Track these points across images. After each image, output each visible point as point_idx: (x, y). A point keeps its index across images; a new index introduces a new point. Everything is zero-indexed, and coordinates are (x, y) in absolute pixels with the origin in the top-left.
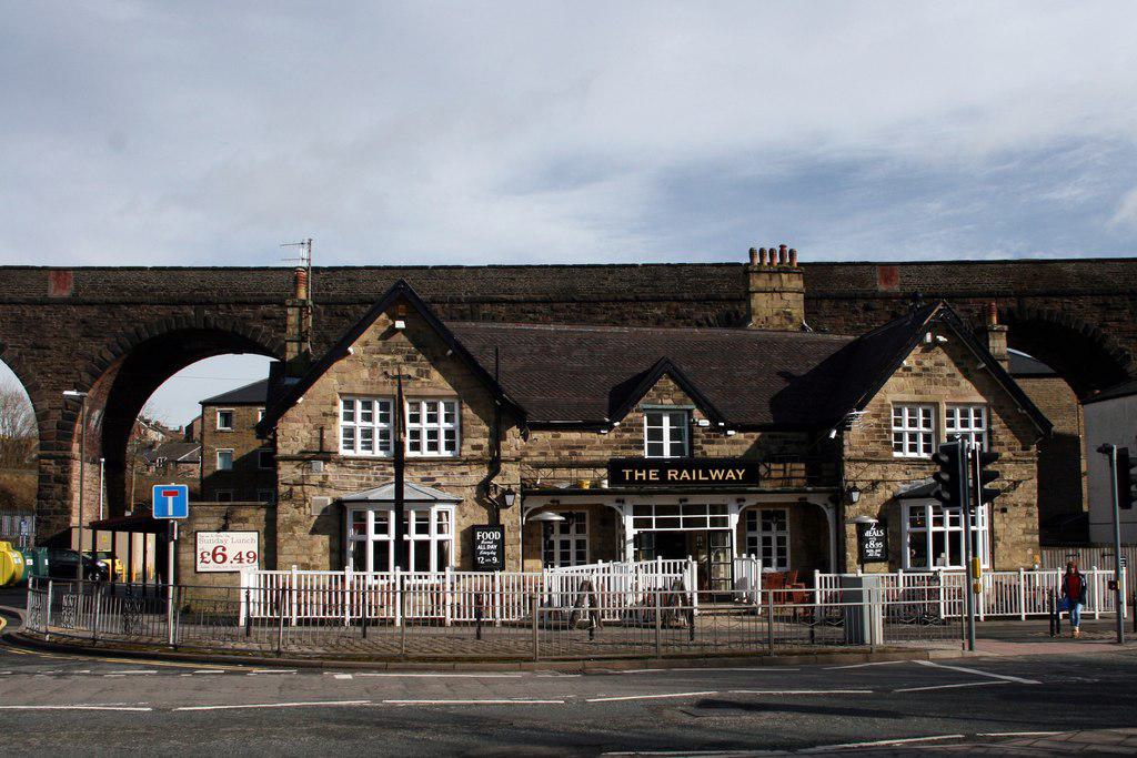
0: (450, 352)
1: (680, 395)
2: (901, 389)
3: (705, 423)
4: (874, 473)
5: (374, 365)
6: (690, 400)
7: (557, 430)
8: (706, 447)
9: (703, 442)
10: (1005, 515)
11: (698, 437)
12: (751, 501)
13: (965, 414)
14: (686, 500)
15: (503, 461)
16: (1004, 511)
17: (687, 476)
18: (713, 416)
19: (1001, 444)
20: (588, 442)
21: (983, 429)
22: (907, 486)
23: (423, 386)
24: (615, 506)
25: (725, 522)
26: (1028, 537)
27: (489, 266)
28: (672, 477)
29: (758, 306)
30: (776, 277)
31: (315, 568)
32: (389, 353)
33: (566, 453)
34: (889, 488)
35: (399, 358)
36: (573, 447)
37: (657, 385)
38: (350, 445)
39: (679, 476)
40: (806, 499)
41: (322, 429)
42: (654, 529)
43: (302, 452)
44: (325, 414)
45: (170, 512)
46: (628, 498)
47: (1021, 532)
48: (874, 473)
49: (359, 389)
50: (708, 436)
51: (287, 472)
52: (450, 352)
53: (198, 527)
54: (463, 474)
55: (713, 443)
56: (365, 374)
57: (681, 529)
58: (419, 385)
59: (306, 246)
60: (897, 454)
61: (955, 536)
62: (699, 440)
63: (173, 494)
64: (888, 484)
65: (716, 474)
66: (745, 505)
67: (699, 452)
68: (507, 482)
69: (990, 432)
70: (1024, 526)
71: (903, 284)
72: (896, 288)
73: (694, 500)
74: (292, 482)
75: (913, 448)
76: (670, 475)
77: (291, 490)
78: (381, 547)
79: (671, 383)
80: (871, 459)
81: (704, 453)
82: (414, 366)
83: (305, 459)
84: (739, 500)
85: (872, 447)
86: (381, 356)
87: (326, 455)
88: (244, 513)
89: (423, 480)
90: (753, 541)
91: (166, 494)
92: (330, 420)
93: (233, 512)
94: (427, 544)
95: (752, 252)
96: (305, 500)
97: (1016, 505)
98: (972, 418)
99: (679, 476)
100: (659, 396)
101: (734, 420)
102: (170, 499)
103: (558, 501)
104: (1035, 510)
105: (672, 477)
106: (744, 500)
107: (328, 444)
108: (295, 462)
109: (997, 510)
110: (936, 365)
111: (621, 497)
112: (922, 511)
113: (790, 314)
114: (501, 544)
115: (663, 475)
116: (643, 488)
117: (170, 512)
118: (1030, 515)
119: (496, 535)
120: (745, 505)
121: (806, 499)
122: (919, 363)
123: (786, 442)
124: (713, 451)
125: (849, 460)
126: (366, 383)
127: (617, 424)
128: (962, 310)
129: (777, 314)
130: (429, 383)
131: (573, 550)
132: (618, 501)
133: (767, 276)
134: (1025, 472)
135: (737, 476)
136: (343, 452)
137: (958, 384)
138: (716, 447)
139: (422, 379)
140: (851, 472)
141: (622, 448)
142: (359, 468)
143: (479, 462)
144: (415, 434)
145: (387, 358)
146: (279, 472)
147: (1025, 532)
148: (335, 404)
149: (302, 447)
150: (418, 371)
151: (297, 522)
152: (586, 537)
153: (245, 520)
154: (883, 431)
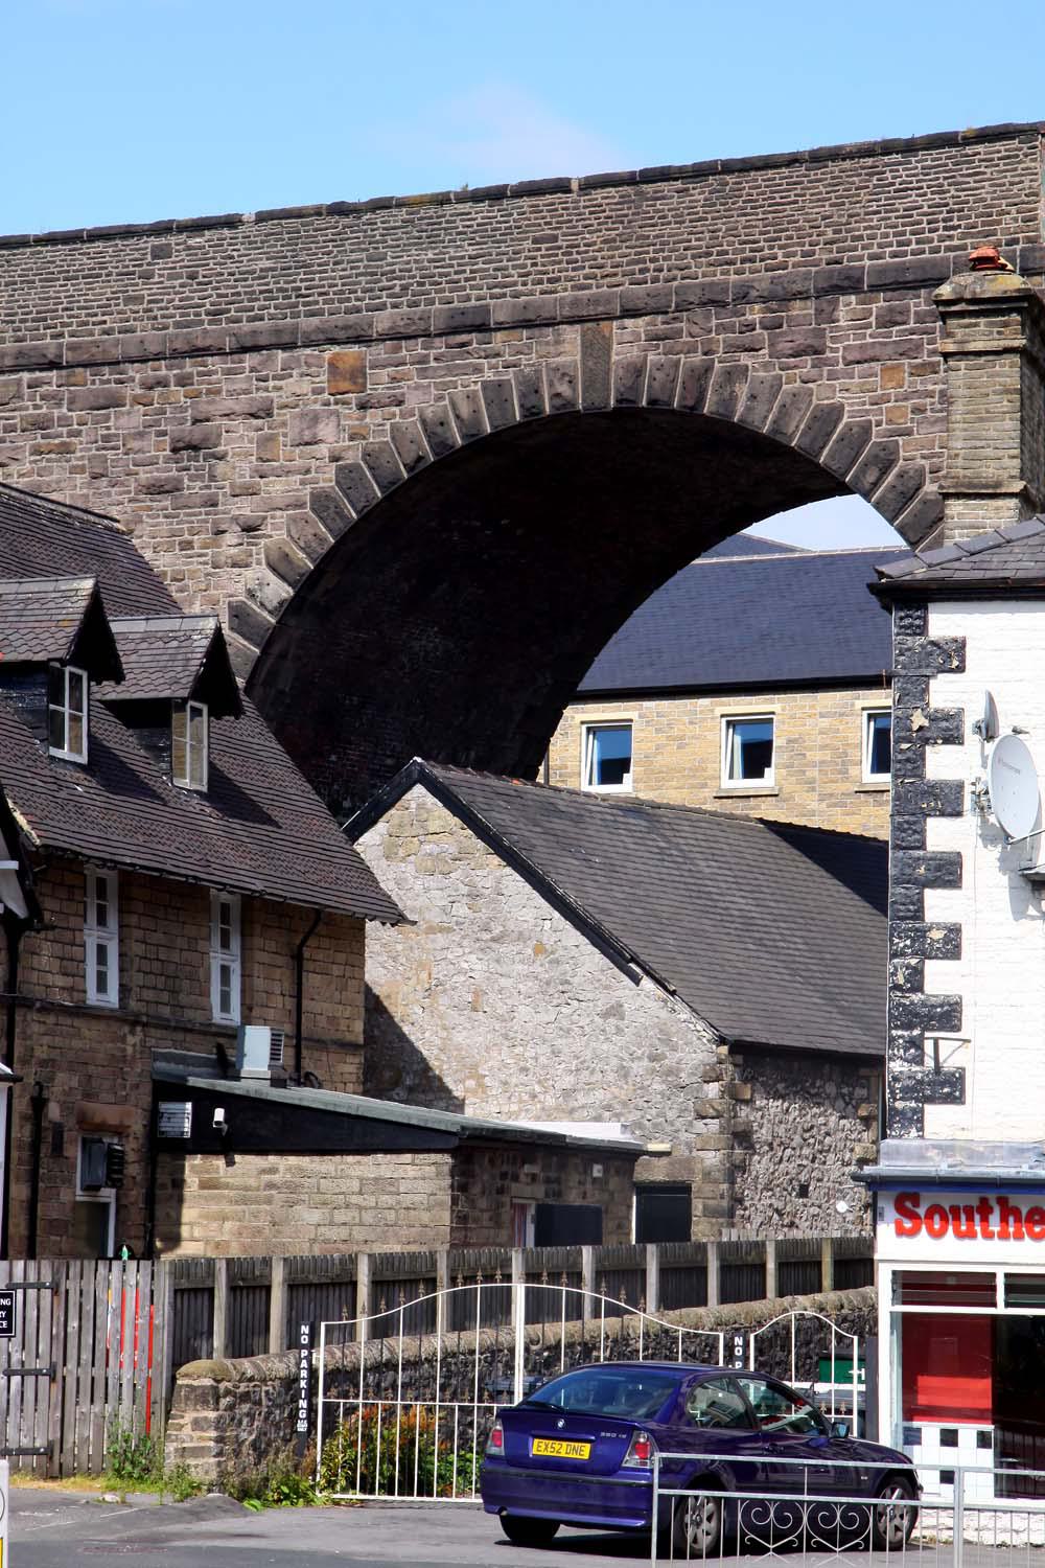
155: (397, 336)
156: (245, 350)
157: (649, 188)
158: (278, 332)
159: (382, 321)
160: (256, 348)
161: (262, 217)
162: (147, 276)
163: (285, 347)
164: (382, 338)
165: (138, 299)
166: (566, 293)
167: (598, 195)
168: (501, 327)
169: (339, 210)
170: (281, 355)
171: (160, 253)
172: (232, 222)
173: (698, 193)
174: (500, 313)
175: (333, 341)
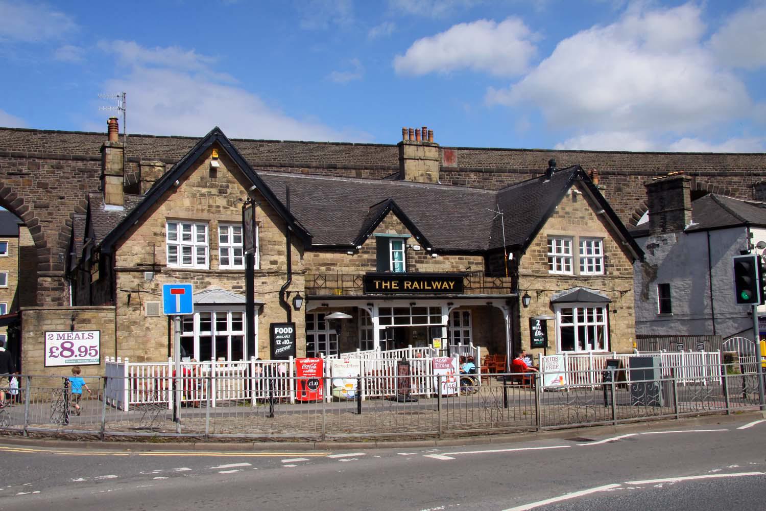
0: (254, 187)
1: (401, 227)
2: (552, 227)
3: (417, 247)
4: (538, 285)
5: (194, 196)
6: (407, 230)
7: (316, 251)
8: (418, 266)
9: (416, 262)
10: (616, 314)
11: (412, 258)
12: (457, 304)
13: (589, 245)
14: (415, 304)
15: (294, 273)
16: (615, 311)
17: (417, 286)
18: (424, 242)
19: (612, 266)
20: (338, 260)
21: (601, 255)
22: (558, 294)
23: (232, 214)
24: (366, 308)
25: (439, 320)
26: (629, 330)
27: (173, 137)
28: (407, 286)
29: (409, 169)
30: (421, 148)
31: (149, 360)
32: (205, 187)
33: (323, 268)
34: (547, 296)
35: (214, 191)
36: (328, 264)
37: (385, 219)
38: (174, 259)
39: (412, 286)
40: (491, 303)
41: (154, 246)
42: (393, 325)
43: (139, 265)
44: (155, 234)
45: (178, 309)
46: (375, 302)
47: (625, 326)
48: (538, 285)
49: (182, 215)
50: (420, 258)
51: (124, 281)
52: (254, 187)
53: (45, 328)
54: (263, 283)
55: (422, 262)
56: (187, 202)
57: (411, 325)
58: (229, 213)
59: (121, 98)
60: (550, 272)
61: (591, 329)
62: (414, 260)
63: (181, 291)
64: (546, 292)
65: (436, 285)
66: (453, 307)
67: (414, 269)
68: (297, 290)
69: (605, 258)
70: (626, 322)
71: (459, 162)
72: (455, 165)
73: (420, 304)
74: (129, 289)
75: (559, 268)
76: (406, 285)
77: (129, 296)
78: (205, 341)
79: (395, 218)
80: (536, 276)
81: (417, 270)
82: (225, 197)
83: (139, 269)
84: (450, 304)
85: (536, 267)
86: (200, 189)
87: (156, 268)
88: (87, 315)
89: (234, 288)
90: (457, 334)
91: (174, 292)
92: (159, 238)
93: (77, 315)
94: (225, 338)
95: (404, 131)
96: (141, 305)
97: (622, 308)
98: (593, 248)
99: (412, 286)
100: (387, 228)
101: (436, 246)
102: (178, 296)
103: (327, 305)
104: (633, 311)
105: (407, 286)
106: (452, 304)
107: (160, 259)
108: (131, 273)
109: (611, 311)
110: (574, 210)
111: (371, 301)
112: (570, 311)
113: (429, 175)
114: (293, 337)
115: (401, 285)
116: (389, 294)
117: (178, 309)
118: (630, 315)
119: (290, 330)
120: (453, 307)
121: (491, 303)
122: (563, 209)
123: (469, 263)
124: (423, 268)
125: (524, 276)
126: (188, 209)
127: (359, 247)
128: (497, 181)
129: (422, 175)
130: (237, 211)
131: (327, 343)
132: (369, 304)
133: (415, 148)
134: (627, 285)
135: (449, 286)
136: (171, 266)
137: (586, 224)
138: (424, 265)
139: (232, 208)
140: (523, 283)
141: (363, 265)
142: (183, 278)
143: (276, 273)
144: (225, 251)
145: (204, 190)
146: (118, 281)
147: (629, 327)
148: (164, 226)
149: (139, 261)
150: (228, 201)
151: (135, 323)
152: (470, 329)
153: (87, 321)
154: (542, 256)
155: (317, 168)
156: (282, 167)
157: (369, 147)
158: (290, 164)
159: (314, 164)
160: (285, 167)
161: (285, 142)
162: (258, 150)
163: (291, 167)
164: (313, 167)
165: (256, 154)
166: (352, 163)
167: (358, 147)
168: (339, 168)
169: (302, 142)
170: (290, 168)
171: (260, 146)
172: (278, 142)
173: (379, 149)
174: (339, 165)
175: (302, 167)
